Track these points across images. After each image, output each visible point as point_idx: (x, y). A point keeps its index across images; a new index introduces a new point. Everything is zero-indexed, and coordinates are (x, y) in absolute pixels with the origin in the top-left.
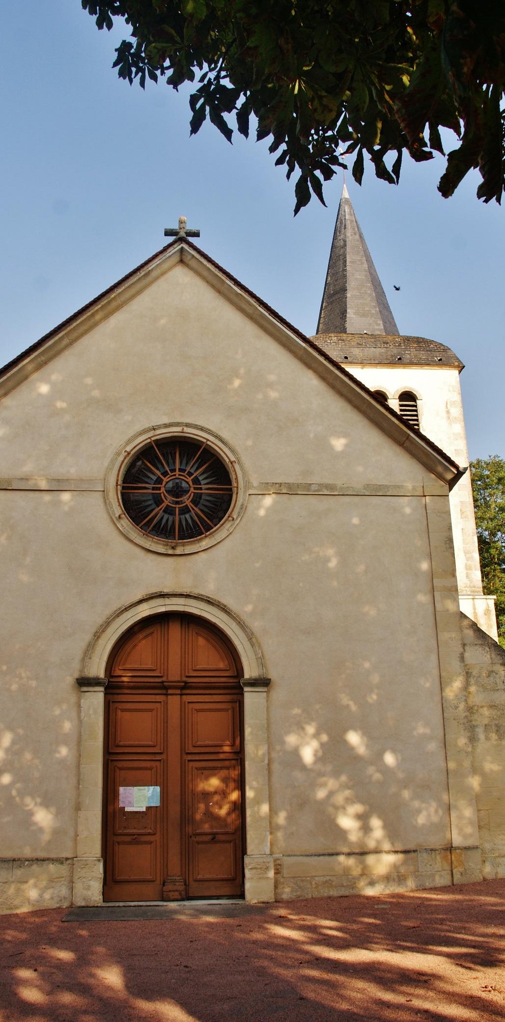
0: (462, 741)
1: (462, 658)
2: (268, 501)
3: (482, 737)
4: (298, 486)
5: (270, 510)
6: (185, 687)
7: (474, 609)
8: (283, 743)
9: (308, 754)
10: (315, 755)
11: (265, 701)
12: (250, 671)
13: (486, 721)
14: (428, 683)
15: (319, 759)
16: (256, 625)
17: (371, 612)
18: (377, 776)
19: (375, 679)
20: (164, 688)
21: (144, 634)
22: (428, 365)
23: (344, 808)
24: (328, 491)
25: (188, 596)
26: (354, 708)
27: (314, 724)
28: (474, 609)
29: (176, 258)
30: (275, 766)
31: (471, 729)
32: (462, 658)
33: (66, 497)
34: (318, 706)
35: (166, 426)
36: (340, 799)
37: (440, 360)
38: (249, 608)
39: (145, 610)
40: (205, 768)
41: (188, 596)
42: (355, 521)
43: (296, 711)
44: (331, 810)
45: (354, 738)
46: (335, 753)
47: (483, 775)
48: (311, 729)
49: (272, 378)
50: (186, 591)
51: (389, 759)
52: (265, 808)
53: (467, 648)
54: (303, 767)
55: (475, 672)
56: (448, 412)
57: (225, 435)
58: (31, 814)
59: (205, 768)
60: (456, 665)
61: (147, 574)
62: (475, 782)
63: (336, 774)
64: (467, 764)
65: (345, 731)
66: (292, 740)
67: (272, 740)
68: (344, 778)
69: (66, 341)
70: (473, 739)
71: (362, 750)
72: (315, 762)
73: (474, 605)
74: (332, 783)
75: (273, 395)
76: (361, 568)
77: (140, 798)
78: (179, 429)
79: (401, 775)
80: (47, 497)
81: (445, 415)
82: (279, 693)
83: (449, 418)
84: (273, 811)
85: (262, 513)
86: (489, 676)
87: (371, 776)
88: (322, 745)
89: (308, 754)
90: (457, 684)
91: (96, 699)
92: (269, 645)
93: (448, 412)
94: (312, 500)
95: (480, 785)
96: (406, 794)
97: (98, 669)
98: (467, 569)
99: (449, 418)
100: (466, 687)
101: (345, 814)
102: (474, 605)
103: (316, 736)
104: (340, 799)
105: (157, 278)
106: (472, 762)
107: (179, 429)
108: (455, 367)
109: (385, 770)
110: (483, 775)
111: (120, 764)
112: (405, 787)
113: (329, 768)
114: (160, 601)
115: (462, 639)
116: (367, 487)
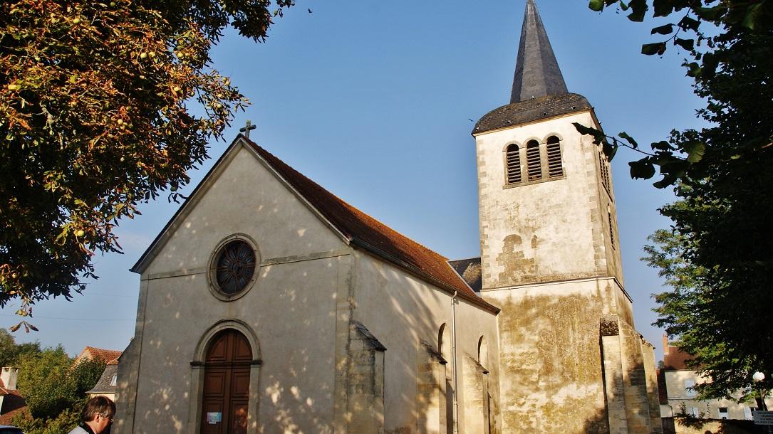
0: (343, 393)
1: (348, 347)
2: (268, 268)
3: (354, 391)
4: (281, 259)
5: (269, 273)
6: (233, 365)
7: (598, 287)
8: (265, 392)
9: (275, 398)
10: (278, 398)
11: (258, 372)
12: (255, 357)
13: (358, 382)
14: (330, 361)
15: (280, 400)
16: (259, 333)
17: (307, 323)
18: (303, 411)
19: (306, 359)
20: (224, 365)
21: (220, 340)
22: (565, 113)
23: (287, 426)
24: (295, 260)
25: (233, 321)
26: (295, 375)
27: (278, 382)
28: (598, 287)
29: (240, 146)
30: (261, 404)
31: (348, 386)
32: (348, 347)
33: (194, 277)
34: (280, 374)
35: (231, 236)
36: (286, 421)
37: (574, 108)
38: (256, 325)
39: (218, 329)
40: (238, 404)
41: (233, 321)
42: (305, 274)
43: (272, 376)
44: (282, 427)
45: (294, 390)
46: (286, 396)
47: (353, 412)
48: (277, 386)
49: (275, 201)
50: (232, 318)
51: (309, 402)
52: (255, 424)
53: (352, 341)
54: (272, 404)
55: (354, 355)
56: (582, 145)
57: (253, 237)
58: (174, 423)
59: (238, 404)
60: (344, 351)
61: (218, 311)
62: (349, 416)
63: (285, 409)
64: (344, 405)
65: (291, 386)
66: (269, 390)
67: (260, 391)
68: (288, 411)
69: (195, 201)
70: (349, 393)
71: (297, 397)
72: (277, 403)
73: (598, 284)
74: (283, 413)
75: (276, 210)
76: (305, 300)
77: (214, 417)
78: (234, 237)
79: (313, 411)
80: (187, 278)
81: (580, 148)
82: (265, 368)
83: (582, 149)
84: (258, 426)
85: (265, 275)
86: (361, 357)
87: (300, 411)
88: (281, 393)
89: (275, 398)
90: (344, 362)
91: (197, 372)
92: (264, 343)
93: (582, 145)
94: (287, 266)
95: (351, 418)
96: (315, 420)
97: (200, 358)
98: (595, 258)
99: (582, 149)
100: (348, 364)
101: (288, 430)
102: (598, 284)
103: (279, 388)
104: (286, 421)
105: (232, 159)
106: (347, 406)
107: (234, 237)
108: (588, 110)
109: (307, 408)
110: (353, 412)
111: (210, 402)
112: (315, 417)
113: (282, 406)
114: (223, 324)
115: (349, 336)
116: (311, 255)
